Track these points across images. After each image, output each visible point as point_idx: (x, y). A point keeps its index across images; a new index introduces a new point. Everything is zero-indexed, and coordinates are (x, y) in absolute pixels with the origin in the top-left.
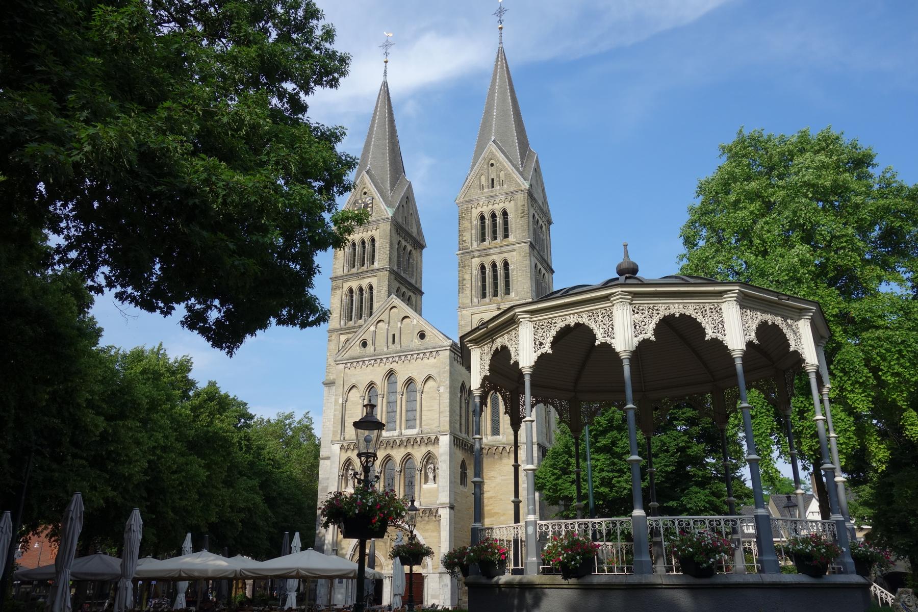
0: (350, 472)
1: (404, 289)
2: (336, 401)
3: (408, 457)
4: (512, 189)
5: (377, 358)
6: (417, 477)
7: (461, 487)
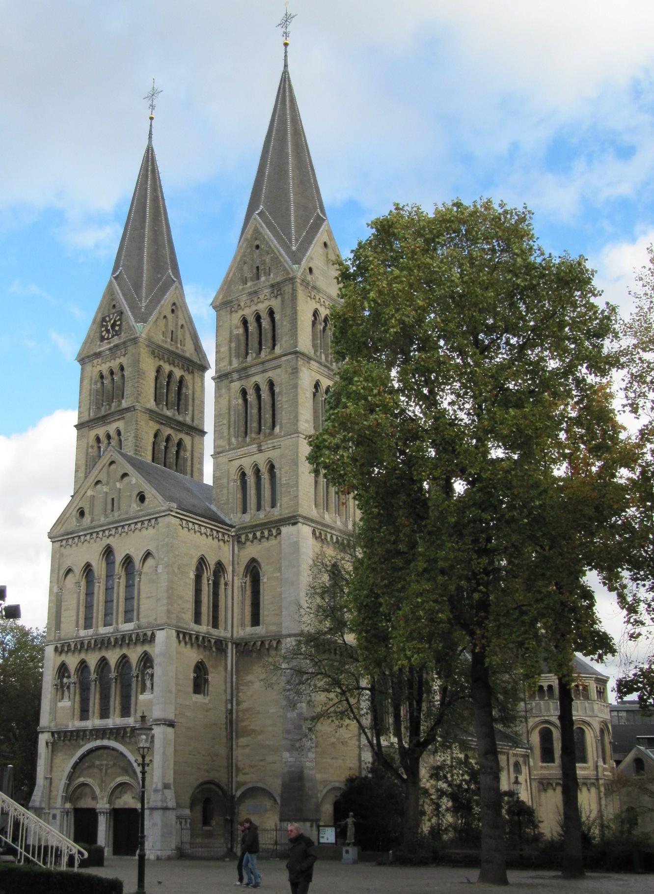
1: (167, 431)
4: (279, 279)
5: (93, 532)
6: (134, 685)
7: (199, 698)
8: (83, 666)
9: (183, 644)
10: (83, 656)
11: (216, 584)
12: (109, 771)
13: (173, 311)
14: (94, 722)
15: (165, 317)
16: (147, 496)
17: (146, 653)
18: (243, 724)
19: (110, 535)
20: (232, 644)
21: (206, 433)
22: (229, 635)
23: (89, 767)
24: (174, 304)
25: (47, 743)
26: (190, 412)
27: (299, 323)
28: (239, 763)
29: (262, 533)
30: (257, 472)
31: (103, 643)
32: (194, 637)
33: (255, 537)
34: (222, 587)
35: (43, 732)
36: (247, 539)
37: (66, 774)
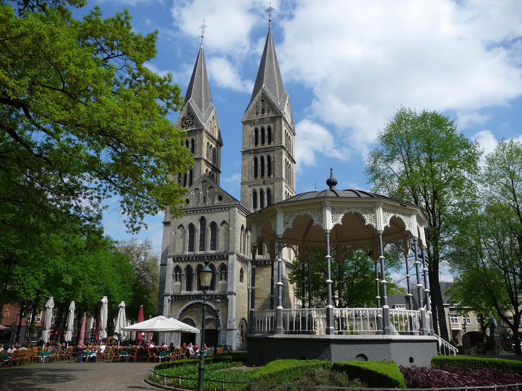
0: (178, 273)
2: (171, 233)
5: (195, 211)
7: (240, 283)
8: (189, 268)
10: (188, 263)
16: (224, 197)
17: (223, 264)
22: (249, 258)
23: (191, 311)
30: (262, 192)
35: (166, 296)
37: (179, 314)
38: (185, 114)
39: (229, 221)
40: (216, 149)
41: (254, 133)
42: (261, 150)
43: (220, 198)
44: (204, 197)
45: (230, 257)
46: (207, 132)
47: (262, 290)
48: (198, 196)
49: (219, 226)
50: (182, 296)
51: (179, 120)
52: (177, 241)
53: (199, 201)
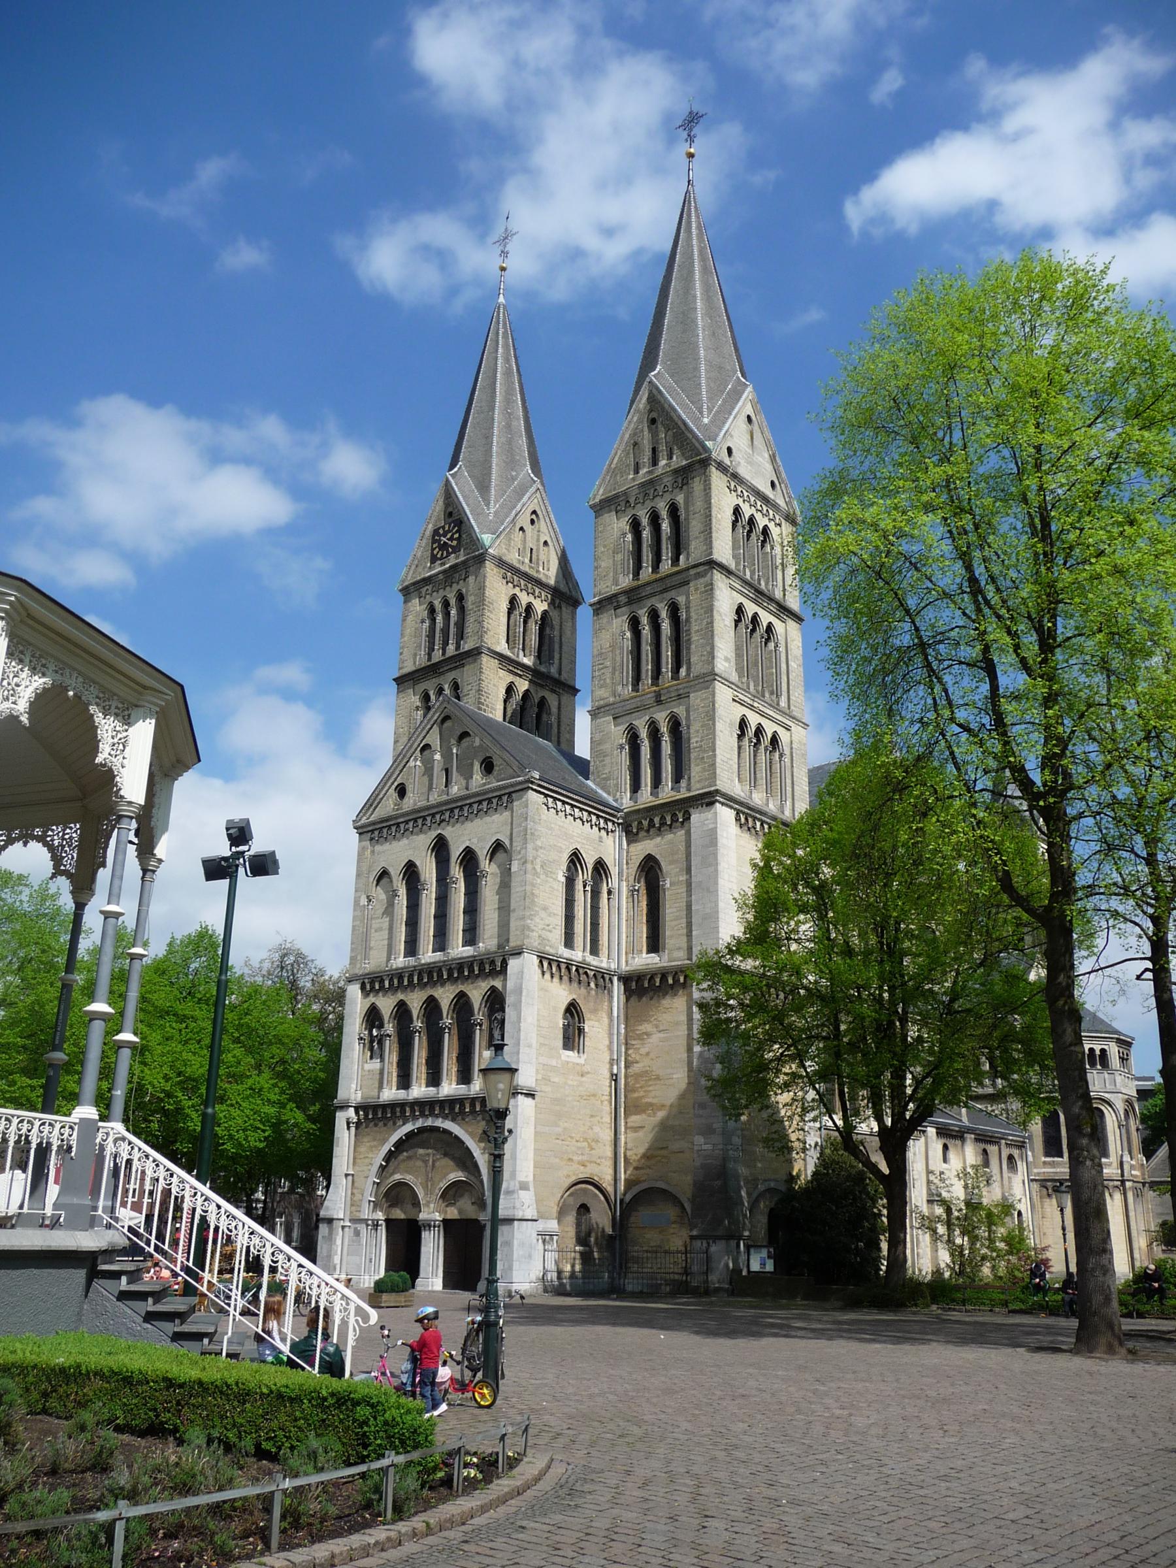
0: (375, 1033)
3: (462, 1004)
5: (418, 819)
8: (402, 1011)
9: (547, 976)
10: (401, 996)
11: (596, 894)
12: (437, 1164)
13: (532, 522)
14: (419, 1090)
15: (521, 529)
16: (497, 762)
17: (493, 989)
18: (636, 1095)
19: (442, 821)
20: (619, 979)
21: (578, 691)
22: (613, 966)
23: (409, 1158)
24: (534, 512)
25: (348, 1123)
26: (556, 661)
27: (714, 520)
28: (629, 1153)
29: (663, 818)
31: (431, 975)
32: (563, 966)
33: (651, 824)
34: (605, 895)
36: (640, 828)
38: (438, 519)
39: (511, 839)
40: (554, 614)
41: (629, 537)
42: (649, 590)
43: (488, 767)
44: (447, 771)
45: (513, 964)
46: (501, 563)
47: (658, 1078)
48: (428, 771)
49: (484, 864)
50: (384, 1107)
51: (424, 541)
52: (375, 924)
53: (430, 788)
